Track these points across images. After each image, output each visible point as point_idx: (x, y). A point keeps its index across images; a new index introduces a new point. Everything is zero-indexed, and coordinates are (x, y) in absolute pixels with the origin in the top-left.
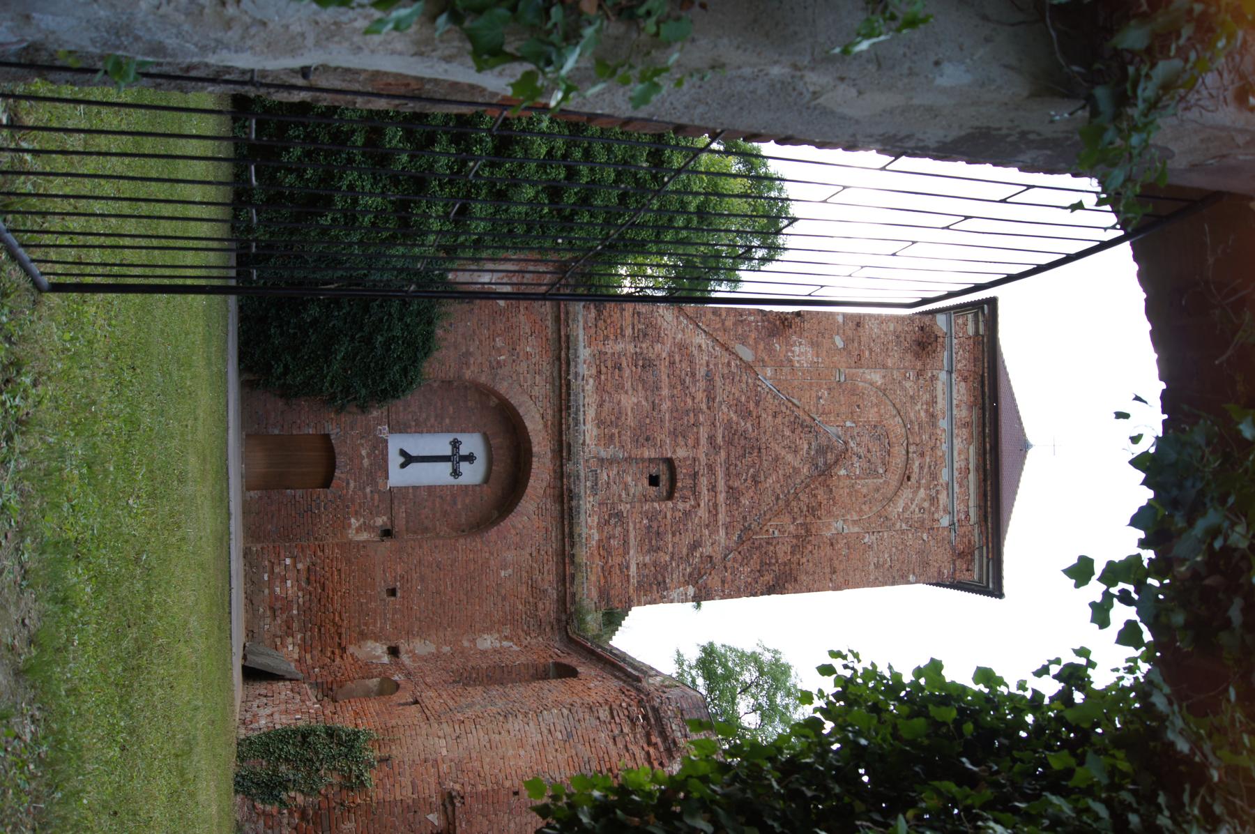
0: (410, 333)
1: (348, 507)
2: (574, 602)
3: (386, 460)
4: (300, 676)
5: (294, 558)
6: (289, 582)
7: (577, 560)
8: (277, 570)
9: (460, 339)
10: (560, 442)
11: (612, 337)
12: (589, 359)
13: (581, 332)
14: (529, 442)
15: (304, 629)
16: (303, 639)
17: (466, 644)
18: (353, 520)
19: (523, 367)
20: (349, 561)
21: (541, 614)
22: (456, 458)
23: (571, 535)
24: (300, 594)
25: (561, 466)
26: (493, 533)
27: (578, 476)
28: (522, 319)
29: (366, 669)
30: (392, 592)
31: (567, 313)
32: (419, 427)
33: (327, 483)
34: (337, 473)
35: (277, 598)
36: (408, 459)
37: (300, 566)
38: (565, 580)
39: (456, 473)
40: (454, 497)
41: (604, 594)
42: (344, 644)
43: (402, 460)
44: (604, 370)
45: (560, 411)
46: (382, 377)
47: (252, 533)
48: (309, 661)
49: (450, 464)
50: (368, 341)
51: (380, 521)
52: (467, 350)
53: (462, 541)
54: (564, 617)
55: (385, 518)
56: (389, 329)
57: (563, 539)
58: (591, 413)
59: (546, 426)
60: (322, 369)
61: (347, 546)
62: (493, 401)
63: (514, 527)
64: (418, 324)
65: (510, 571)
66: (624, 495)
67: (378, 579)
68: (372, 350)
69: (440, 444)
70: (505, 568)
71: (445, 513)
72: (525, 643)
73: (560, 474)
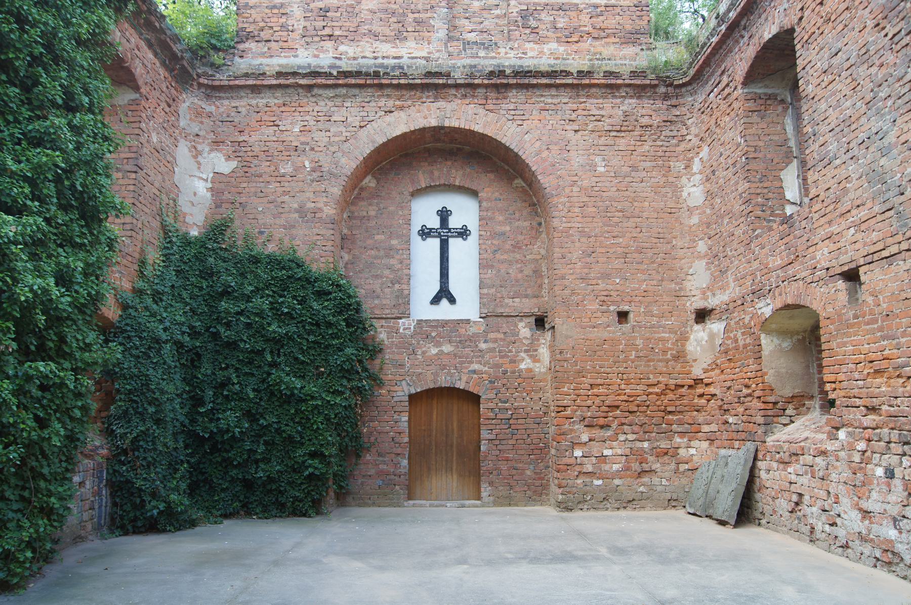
0: (268, 286)
1: (505, 373)
2: (641, 74)
3: (444, 323)
4: (751, 446)
5: (574, 445)
6: (607, 452)
7: (585, 69)
8: (589, 468)
9: (281, 221)
10: (424, 87)
11: (283, 20)
12: (312, 50)
13: (276, 61)
14: (423, 130)
15: (669, 434)
16: (682, 434)
17: (695, 220)
18: (523, 366)
19: (321, 138)
20: (580, 373)
21: (656, 120)
22: (444, 232)
23: (552, 74)
24: (622, 437)
25: (457, 86)
26: (546, 181)
27: (471, 66)
28: (255, 138)
29: (728, 354)
30: (623, 316)
31: (246, 75)
32: (402, 279)
33: (474, 399)
34: (461, 385)
35: (628, 469)
36: (444, 294)
37: (585, 438)
38: (612, 86)
39: (463, 233)
40: (494, 235)
41: (632, 38)
42: (691, 382)
43: (444, 302)
44: (327, 31)
45: (381, 86)
46: (329, 325)
47: (536, 492)
48: (714, 427)
49: (451, 240)
50: (277, 342)
51: (524, 330)
52: (297, 211)
53: (556, 223)
54: (662, 89)
55: (521, 325)
56: (260, 314)
57: (557, 86)
58: (386, 49)
59: (401, 108)
60: (316, 407)
61: (558, 376)
62: (369, 182)
63: (539, 153)
64: (257, 276)
65: (598, 159)
66: (498, 12)
67: (606, 335)
68: (291, 338)
69: (426, 253)
70: (593, 167)
71: (516, 247)
72: (695, 141)
73: (468, 88)
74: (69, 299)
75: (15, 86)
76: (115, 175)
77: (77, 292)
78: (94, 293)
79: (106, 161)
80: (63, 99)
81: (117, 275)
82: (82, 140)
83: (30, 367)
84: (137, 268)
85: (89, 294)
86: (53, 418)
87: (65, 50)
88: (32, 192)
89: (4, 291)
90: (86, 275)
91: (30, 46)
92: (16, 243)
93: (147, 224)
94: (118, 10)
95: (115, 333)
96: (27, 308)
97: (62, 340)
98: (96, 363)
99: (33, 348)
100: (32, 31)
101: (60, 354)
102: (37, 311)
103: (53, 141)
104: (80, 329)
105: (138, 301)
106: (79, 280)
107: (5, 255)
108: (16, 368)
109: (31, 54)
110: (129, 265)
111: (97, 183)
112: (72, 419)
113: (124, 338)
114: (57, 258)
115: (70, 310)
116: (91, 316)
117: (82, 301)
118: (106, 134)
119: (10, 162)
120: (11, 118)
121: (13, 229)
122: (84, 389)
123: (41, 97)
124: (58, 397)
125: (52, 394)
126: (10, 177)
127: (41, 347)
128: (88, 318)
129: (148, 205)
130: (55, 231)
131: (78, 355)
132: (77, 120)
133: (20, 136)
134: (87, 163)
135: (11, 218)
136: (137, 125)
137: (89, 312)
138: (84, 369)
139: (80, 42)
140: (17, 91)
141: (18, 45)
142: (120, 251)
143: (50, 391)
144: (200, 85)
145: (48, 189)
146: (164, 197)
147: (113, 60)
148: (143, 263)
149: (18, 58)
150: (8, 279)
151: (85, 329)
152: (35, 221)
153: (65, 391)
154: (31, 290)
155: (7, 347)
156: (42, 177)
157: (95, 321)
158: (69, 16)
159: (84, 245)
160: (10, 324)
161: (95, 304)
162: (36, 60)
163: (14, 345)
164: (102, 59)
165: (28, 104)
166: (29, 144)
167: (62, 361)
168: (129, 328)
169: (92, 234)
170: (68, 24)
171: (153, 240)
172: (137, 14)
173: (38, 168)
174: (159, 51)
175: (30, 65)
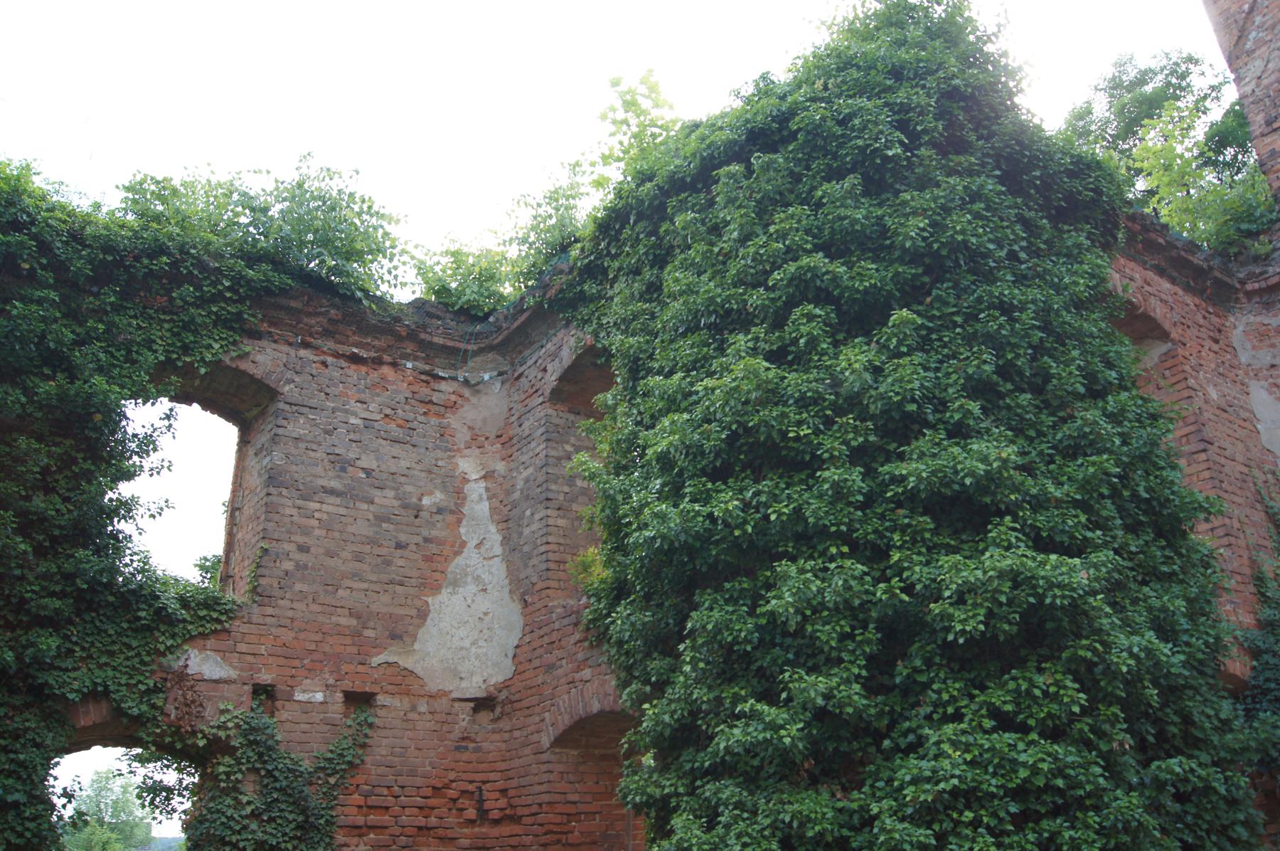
74: (1182, 657)
75: (1023, 391)
76: (1182, 463)
77: (1188, 644)
78: (1212, 640)
79: (1163, 447)
80: (1083, 385)
81: (1228, 607)
82: (1125, 430)
83: (1159, 767)
84: (1253, 589)
85: (1206, 644)
86: (1208, 844)
87: (1065, 323)
88: (1088, 520)
89: (1096, 664)
90: (1191, 616)
91: (1027, 335)
92: (1094, 593)
93: (1246, 520)
94: (1106, 247)
95: (1254, 697)
96: (1132, 681)
97: (1187, 720)
98: (1246, 749)
99: (1151, 739)
100: (1024, 316)
101: (1191, 743)
102: (1146, 684)
103: (1091, 444)
104: (1206, 700)
105: (1272, 639)
106: (1186, 627)
107: (1085, 613)
108: (1138, 772)
109: (1030, 346)
110: (1241, 587)
111: (1163, 481)
112: (1230, 839)
113: (1270, 701)
114: (1145, 601)
115: (1186, 673)
116: (1213, 677)
117: (1200, 656)
118: (1152, 411)
119: (1051, 488)
120: (1032, 433)
121: (1083, 574)
122: (1241, 792)
123: (1059, 393)
124: (1206, 810)
125: (1197, 806)
126: (1056, 508)
127: (1161, 735)
128: (1212, 681)
129: (1238, 492)
130: (1130, 564)
131: (1215, 739)
132: (1111, 403)
133: (1050, 451)
134: (1144, 458)
135: (1077, 561)
136: (1183, 385)
137: (1209, 671)
138: (1232, 761)
139: (1079, 305)
140: (1029, 396)
141: (1013, 340)
142: (1222, 571)
143: (1191, 801)
144: (1249, 295)
145: (1105, 508)
146: (1256, 472)
147: (1127, 309)
148: (1259, 580)
149: (1018, 356)
150: (1098, 645)
151: (1214, 699)
152: (1107, 556)
153: (1214, 798)
154: (1132, 655)
155: (1121, 744)
156: (1095, 495)
157: (1221, 684)
158: (1056, 280)
159: (1174, 573)
160: (1115, 709)
161: (1215, 658)
162: (1039, 349)
163: (1129, 741)
164: (1111, 315)
165: (1046, 408)
166: (1064, 458)
167: (1196, 753)
168: (1273, 685)
169: (1180, 555)
170: (1058, 289)
171: (1262, 542)
172: (1131, 238)
173: (1085, 485)
174: (1175, 274)
175: (1034, 359)
